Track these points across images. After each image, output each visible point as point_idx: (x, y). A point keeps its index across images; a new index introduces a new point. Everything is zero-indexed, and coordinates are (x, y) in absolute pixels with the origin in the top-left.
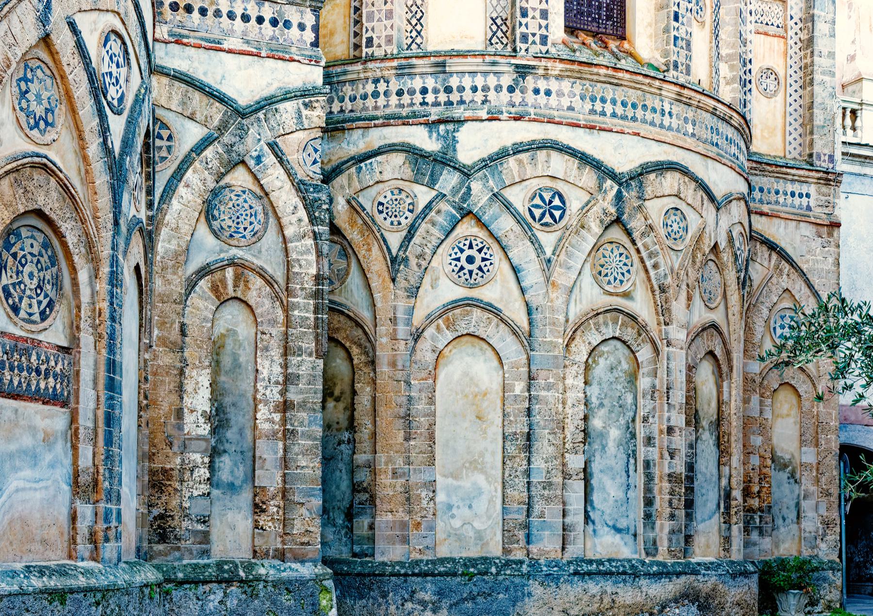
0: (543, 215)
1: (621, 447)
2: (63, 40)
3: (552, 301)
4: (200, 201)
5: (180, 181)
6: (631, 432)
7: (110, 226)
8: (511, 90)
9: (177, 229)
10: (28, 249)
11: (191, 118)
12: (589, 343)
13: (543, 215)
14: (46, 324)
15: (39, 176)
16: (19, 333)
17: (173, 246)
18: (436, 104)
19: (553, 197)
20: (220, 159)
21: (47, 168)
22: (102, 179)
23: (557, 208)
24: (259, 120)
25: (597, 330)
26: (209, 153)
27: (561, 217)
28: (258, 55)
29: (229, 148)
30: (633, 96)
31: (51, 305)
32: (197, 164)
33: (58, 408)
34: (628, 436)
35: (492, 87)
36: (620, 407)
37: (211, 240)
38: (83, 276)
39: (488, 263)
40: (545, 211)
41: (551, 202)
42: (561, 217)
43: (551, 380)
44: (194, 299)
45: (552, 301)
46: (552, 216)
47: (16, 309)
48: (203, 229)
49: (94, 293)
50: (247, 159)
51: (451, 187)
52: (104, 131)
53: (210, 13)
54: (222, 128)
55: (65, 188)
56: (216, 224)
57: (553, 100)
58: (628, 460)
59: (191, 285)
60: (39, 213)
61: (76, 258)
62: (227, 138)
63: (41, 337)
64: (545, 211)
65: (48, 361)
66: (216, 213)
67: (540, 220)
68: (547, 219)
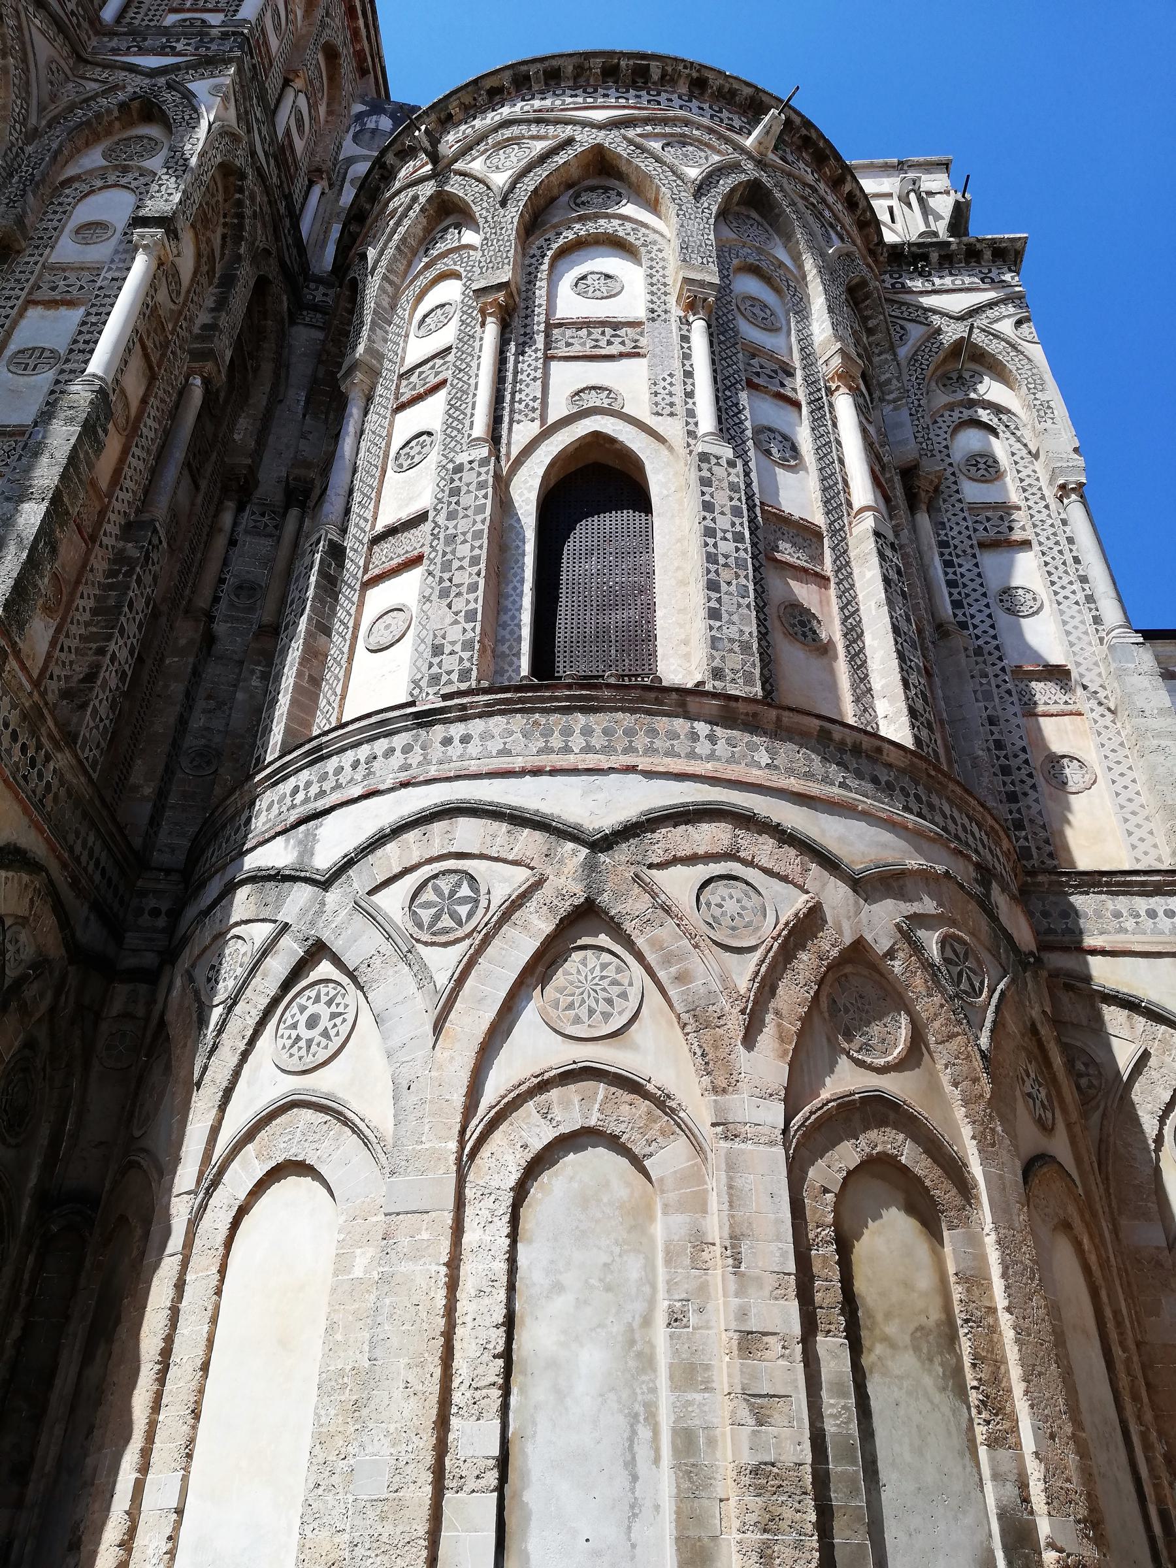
0: (437, 917)
1: (612, 1396)
3: (440, 1068)
6: (639, 1355)
8: (407, 749)
12: (525, 1147)
13: (437, 917)
18: (306, 800)
19: (458, 885)
23: (464, 901)
25: (545, 1116)
27: (470, 915)
30: (627, 719)
34: (632, 1364)
35: (379, 753)
36: (608, 1289)
39: (338, 1020)
40: (442, 910)
41: (453, 893)
42: (470, 915)
43: (425, 1235)
45: (440, 1068)
46: (454, 916)
51: (298, 909)
57: (473, 749)
58: (634, 1432)
64: (442, 910)
67: (432, 925)
68: (446, 922)
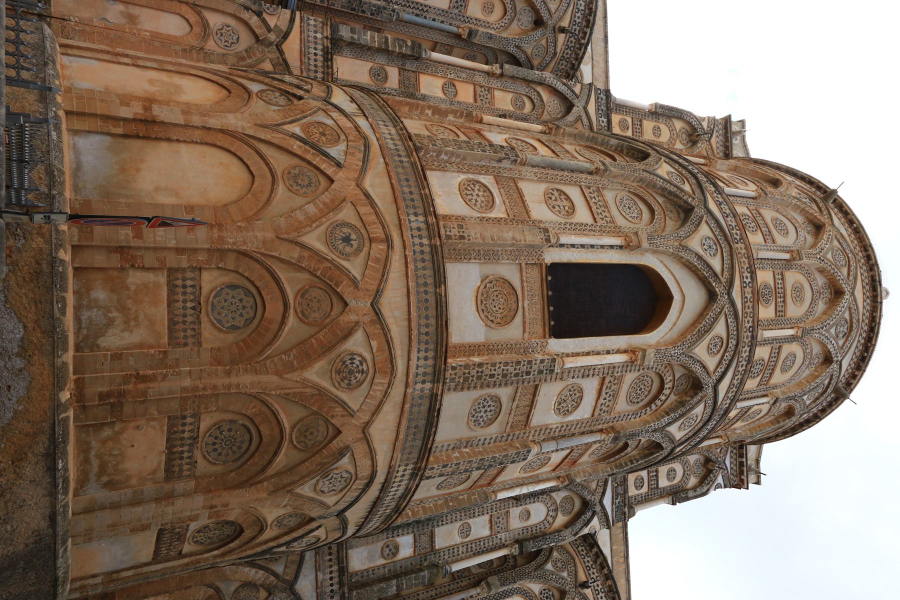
2: (314, 525)
4: (250, 579)
5: (258, 568)
7: (239, 557)
9: (236, 573)
10: (226, 530)
11: (286, 567)
14: (192, 543)
15: (258, 528)
16: (188, 536)
17: (228, 573)
20: (270, 584)
21: (262, 530)
22: (259, 549)
24: (290, 596)
26: (272, 578)
28: (317, 588)
29: (276, 587)
31: (201, 543)
32: (267, 574)
33: (152, 557)
37: (233, 589)
38: (215, 553)
44: (204, 588)
47: (199, 532)
48: (237, 584)
49: (207, 559)
50: (272, 596)
52: (279, 546)
53: (330, 563)
54: (284, 581)
55: (254, 538)
56: (241, 589)
59: (210, 586)
60: (242, 531)
61: (223, 548)
62: (279, 584)
63: (186, 543)
65: (174, 548)
66: (246, 588)
